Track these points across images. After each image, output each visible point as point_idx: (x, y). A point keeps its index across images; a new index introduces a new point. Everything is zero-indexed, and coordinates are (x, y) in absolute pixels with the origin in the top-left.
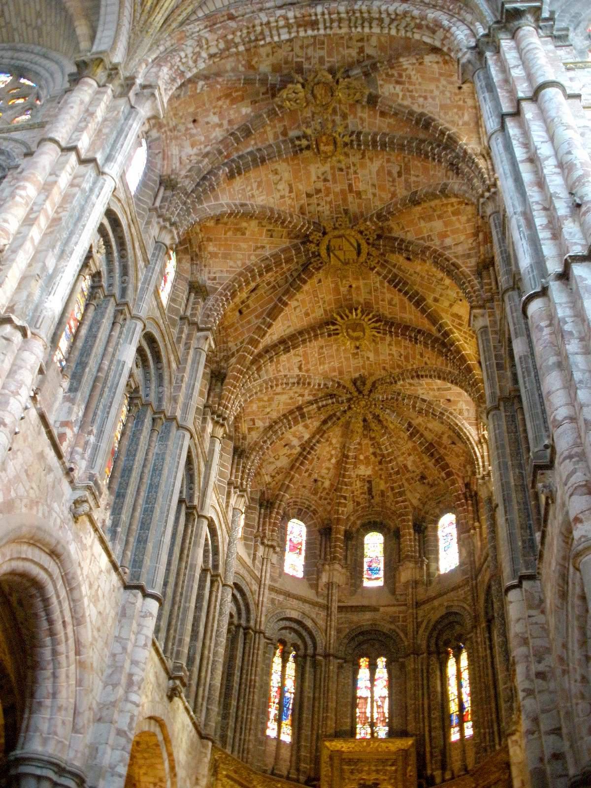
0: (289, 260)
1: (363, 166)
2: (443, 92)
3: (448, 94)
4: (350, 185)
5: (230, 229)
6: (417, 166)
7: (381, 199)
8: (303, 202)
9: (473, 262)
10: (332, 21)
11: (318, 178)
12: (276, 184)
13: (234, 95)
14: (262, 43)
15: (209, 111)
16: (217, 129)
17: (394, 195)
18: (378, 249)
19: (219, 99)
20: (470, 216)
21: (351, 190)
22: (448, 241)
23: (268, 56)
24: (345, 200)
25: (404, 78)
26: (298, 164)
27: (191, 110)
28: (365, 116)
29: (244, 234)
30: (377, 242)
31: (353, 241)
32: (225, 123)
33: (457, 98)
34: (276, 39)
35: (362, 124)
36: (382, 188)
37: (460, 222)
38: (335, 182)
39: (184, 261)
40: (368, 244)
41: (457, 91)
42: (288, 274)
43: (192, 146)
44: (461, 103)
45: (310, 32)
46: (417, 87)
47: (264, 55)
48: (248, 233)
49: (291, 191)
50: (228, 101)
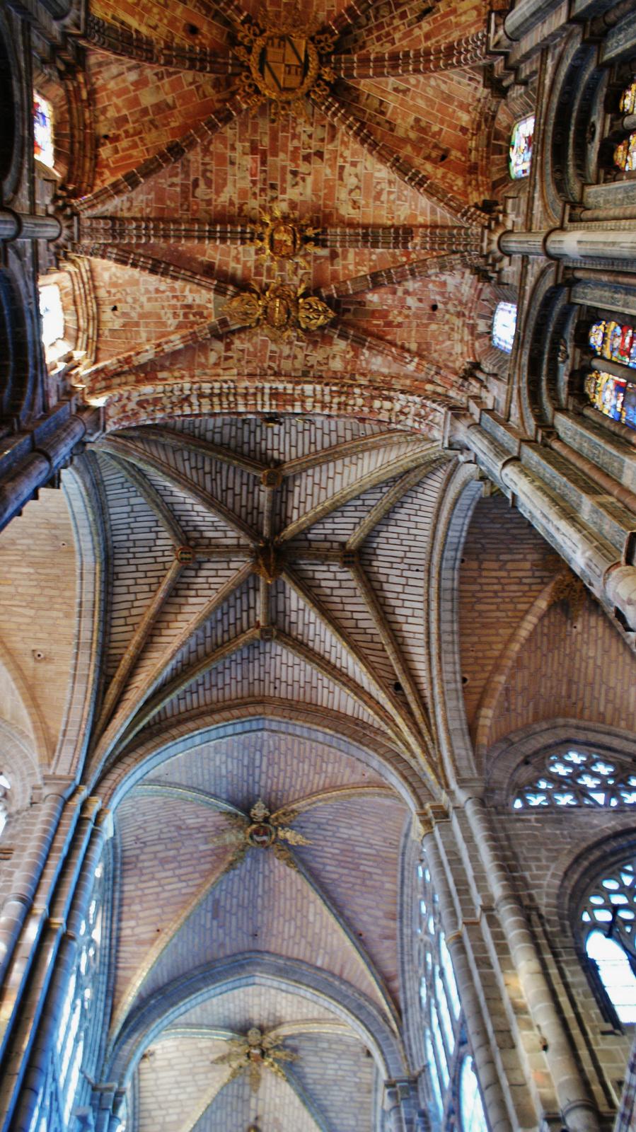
0: (365, 61)
1: (243, 194)
2: (135, 300)
3: (129, 300)
4: (264, 163)
5: (433, 136)
6: (171, 199)
7: (224, 140)
8: (330, 147)
9: (92, 60)
10: (255, 394)
11: (304, 179)
12: (358, 187)
13: (381, 322)
14: (334, 388)
15: (414, 314)
16: (411, 290)
17: (206, 151)
18: (235, 58)
19: (400, 325)
20: (102, 118)
21: (264, 154)
22: (132, 76)
23: (334, 357)
24: (274, 138)
25: (181, 312)
26: (326, 206)
27: (433, 327)
28: (233, 264)
29: (417, 120)
30: (237, 70)
31: (269, 79)
32: (400, 293)
33: (119, 296)
34: (318, 387)
35: (238, 253)
36: (221, 160)
37: (116, 106)
38: (284, 168)
39: (504, 124)
40: (248, 69)
41: (118, 305)
42: (373, 23)
43: (444, 284)
44: (113, 291)
45: (280, 386)
46: (166, 304)
47: (338, 359)
48: (411, 120)
49: (342, 168)
50: (391, 318)
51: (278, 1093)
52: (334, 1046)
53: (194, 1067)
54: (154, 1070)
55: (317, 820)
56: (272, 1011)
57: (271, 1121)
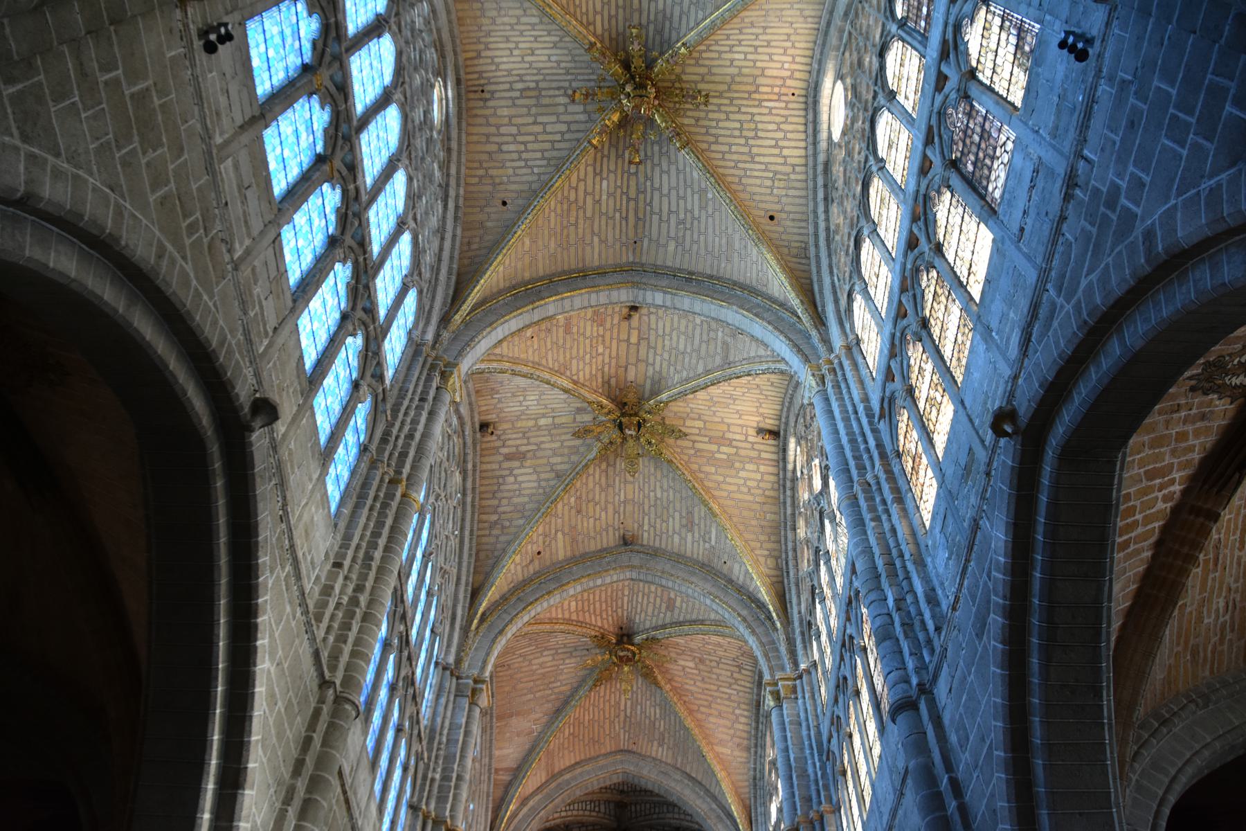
51: (600, 358)
52: (531, 423)
53: (710, 407)
54: (762, 415)
55: (573, 660)
56: (611, 469)
57: (609, 319)
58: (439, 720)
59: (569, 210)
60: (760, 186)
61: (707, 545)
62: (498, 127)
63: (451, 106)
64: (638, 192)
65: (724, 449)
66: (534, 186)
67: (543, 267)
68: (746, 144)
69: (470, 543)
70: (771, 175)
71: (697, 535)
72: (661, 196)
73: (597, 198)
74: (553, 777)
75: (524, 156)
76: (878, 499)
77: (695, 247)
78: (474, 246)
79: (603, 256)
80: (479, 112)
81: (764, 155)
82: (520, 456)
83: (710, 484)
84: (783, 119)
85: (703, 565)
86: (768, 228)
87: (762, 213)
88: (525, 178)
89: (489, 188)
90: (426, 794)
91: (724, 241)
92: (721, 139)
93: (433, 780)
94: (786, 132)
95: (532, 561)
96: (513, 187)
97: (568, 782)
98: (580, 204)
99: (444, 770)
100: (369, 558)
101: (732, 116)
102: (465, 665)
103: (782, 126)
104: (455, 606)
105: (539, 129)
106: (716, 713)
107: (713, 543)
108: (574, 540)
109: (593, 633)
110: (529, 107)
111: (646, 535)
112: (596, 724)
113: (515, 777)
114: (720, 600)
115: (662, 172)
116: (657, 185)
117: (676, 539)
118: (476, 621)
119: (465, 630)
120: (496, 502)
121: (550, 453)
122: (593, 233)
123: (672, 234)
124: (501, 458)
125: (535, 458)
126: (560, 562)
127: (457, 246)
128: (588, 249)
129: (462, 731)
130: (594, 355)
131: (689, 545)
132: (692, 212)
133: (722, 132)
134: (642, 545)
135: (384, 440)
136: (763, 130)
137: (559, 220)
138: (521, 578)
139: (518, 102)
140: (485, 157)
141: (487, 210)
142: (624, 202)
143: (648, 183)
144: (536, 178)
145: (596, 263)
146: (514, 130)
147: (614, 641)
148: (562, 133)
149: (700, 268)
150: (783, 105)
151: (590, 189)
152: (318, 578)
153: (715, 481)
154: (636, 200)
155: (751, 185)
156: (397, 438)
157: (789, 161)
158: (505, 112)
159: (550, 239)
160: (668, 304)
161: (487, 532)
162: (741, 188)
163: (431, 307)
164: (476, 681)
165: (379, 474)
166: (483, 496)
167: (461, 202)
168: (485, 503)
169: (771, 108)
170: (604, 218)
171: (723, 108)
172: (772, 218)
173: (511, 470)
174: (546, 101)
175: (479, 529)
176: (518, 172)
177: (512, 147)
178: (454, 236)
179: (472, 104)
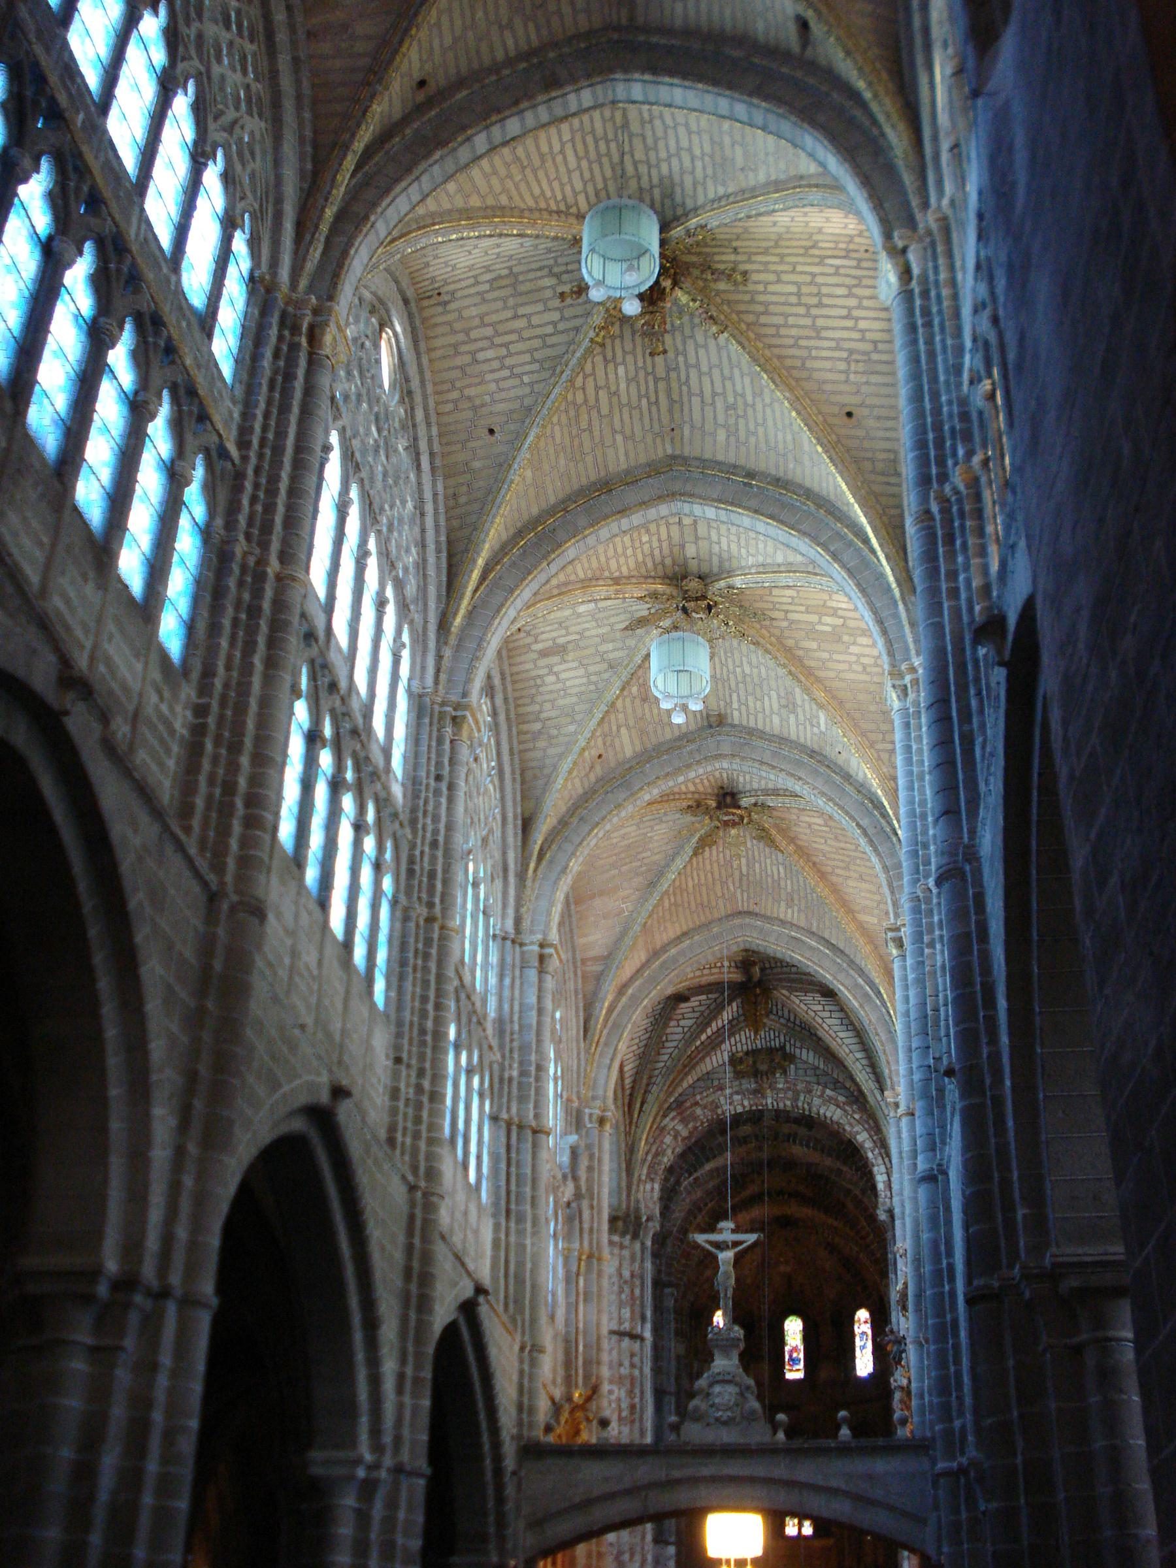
58: (506, 1007)
59: (577, 416)
60: (830, 370)
61: (815, 730)
62: (467, 332)
63: (401, 337)
64: (668, 370)
65: (827, 619)
66: (527, 402)
67: (554, 492)
68: (807, 315)
69: (512, 765)
70: (845, 355)
71: (801, 717)
72: (700, 374)
73: (613, 388)
74: (655, 954)
75: (508, 362)
76: (936, 918)
77: (752, 440)
78: (462, 500)
79: (632, 455)
80: (440, 320)
81: (833, 329)
82: (560, 650)
83: (812, 664)
84: (854, 282)
85: (812, 753)
86: (843, 431)
87: (836, 410)
88: (512, 393)
89: (469, 414)
90: (505, 1100)
91: (789, 437)
92: (772, 308)
93: (510, 1079)
94: (860, 298)
95: (592, 768)
96: (500, 407)
97: (674, 960)
98: (592, 402)
99: (521, 1063)
100: (423, 1032)
101: (785, 277)
102: (526, 924)
103: (854, 290)
104: (504, 853)
105: (520, 323)
106: (856, 875)
107: (823, 728)
108: (643, 733)
109: (685, 804)
110: (504, 300)
111: (736, 713)
112: (704, 889)
113: (607, 967)
114: (836, 804)
115: (697, 346)
116: (692, 361)
117: (776, 720)
118: (532, 865)
119: (521, 877)
120: (537, 707)
121: (598, 640)
122: (614, 431)
123: (721, 419)
124: (534, 656)
125: (578, 647)
126: (629, 760)
127: (442, 510)
128: (610, 452)
129: (534, 1013)
130: (637, 544)
131: (793, 729)
132: (743, 396)
133: (774, 298)
134: (733, 726)
135: (411, 872)
136: (829, 296)
137: (565, 430)
138: (580, 791)
139: (489, 296)
140: (456, 374)
141: (470, 445)
142: (651, 383)
143: (681, 359)
144: (527, 390)
145: (624, 466)
146: (489, 331)
147: (713, 804)
148: (554, 324)
149: (762, 466)
150: (854, 263)
151: (601, 383)
152: (385, 1086)
153: (819, 659)
154: (667, 379)
155: (820, 370)
156: (422, 853)
157: (868, 336)
158: (474, 311)
159: (557, 457)
160: (724, 518)
161: (531, 745)
162: (804, 374)
163: (426, 622)
164: (542, 946)
165: (412, 925)
166: (520, 702)
167: (436, 447)
168: (522, 710)
169: (838, 268)
170: (625, 410)
171: (772, 267)
172: (849, 415)
173: (550, 667)
174: (522, 288)
175: (520, 743)
176: (503, 384)
177: (490, 354)
178: (435, 495)
179: (427, 313)
